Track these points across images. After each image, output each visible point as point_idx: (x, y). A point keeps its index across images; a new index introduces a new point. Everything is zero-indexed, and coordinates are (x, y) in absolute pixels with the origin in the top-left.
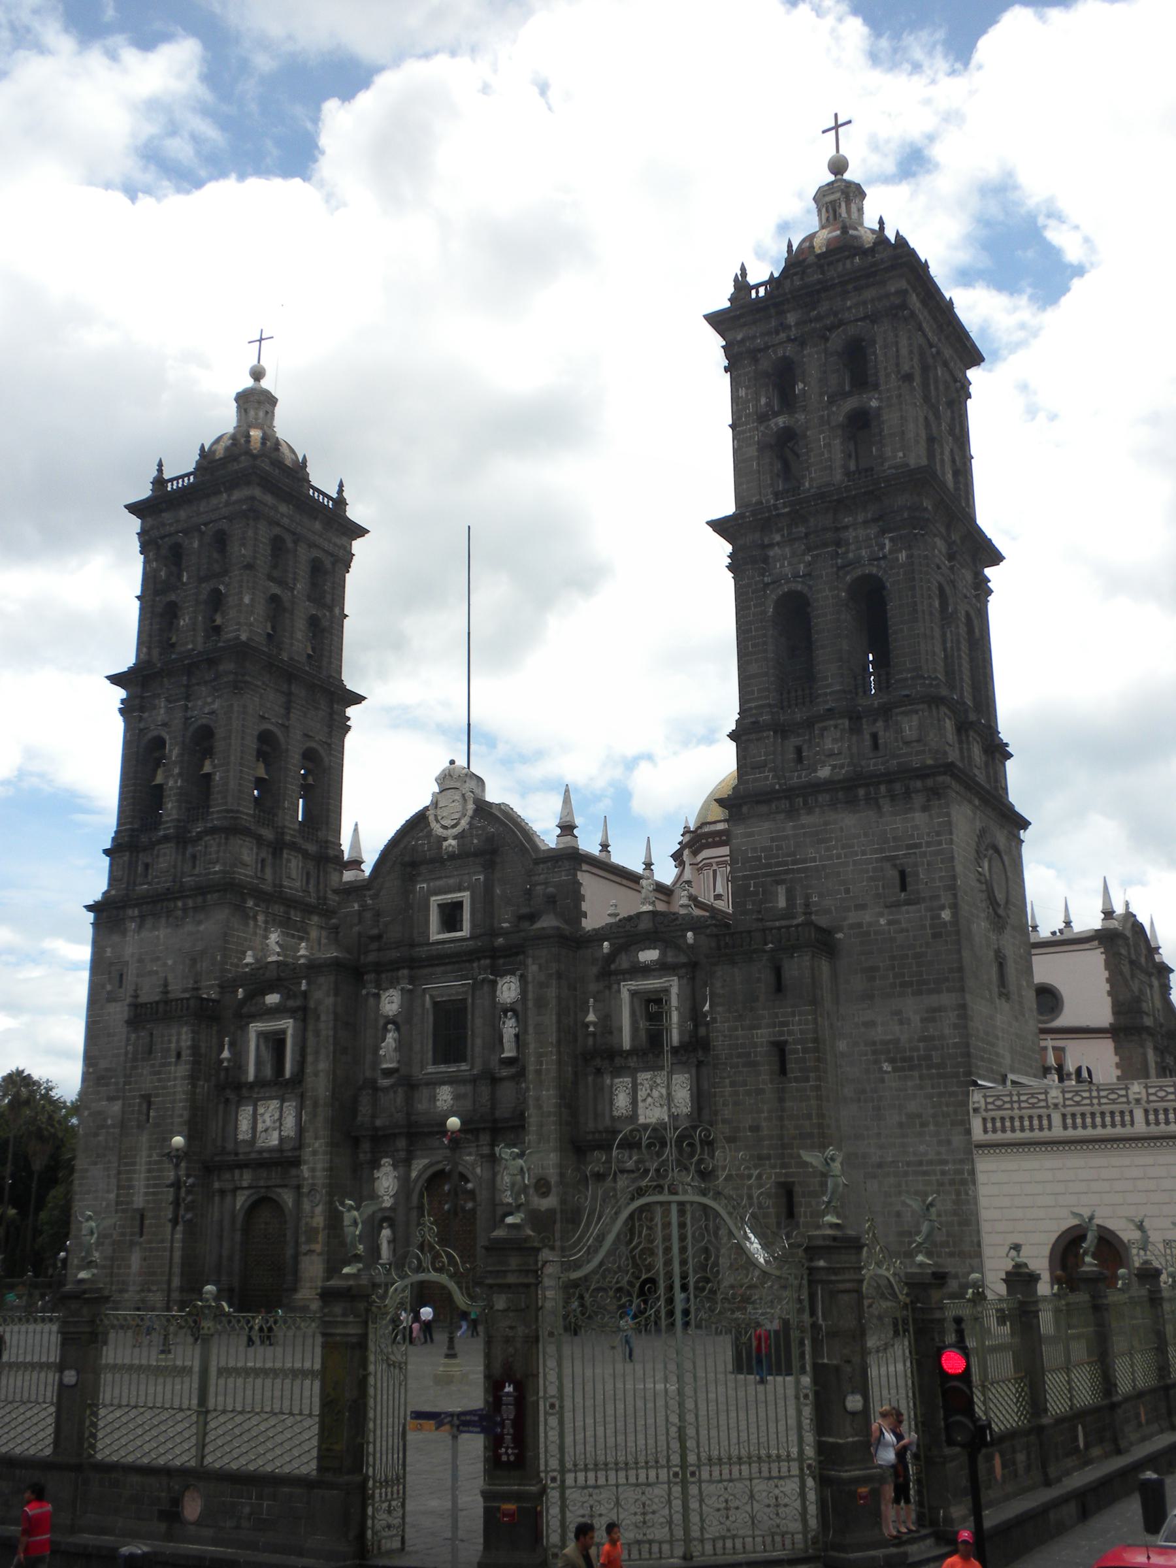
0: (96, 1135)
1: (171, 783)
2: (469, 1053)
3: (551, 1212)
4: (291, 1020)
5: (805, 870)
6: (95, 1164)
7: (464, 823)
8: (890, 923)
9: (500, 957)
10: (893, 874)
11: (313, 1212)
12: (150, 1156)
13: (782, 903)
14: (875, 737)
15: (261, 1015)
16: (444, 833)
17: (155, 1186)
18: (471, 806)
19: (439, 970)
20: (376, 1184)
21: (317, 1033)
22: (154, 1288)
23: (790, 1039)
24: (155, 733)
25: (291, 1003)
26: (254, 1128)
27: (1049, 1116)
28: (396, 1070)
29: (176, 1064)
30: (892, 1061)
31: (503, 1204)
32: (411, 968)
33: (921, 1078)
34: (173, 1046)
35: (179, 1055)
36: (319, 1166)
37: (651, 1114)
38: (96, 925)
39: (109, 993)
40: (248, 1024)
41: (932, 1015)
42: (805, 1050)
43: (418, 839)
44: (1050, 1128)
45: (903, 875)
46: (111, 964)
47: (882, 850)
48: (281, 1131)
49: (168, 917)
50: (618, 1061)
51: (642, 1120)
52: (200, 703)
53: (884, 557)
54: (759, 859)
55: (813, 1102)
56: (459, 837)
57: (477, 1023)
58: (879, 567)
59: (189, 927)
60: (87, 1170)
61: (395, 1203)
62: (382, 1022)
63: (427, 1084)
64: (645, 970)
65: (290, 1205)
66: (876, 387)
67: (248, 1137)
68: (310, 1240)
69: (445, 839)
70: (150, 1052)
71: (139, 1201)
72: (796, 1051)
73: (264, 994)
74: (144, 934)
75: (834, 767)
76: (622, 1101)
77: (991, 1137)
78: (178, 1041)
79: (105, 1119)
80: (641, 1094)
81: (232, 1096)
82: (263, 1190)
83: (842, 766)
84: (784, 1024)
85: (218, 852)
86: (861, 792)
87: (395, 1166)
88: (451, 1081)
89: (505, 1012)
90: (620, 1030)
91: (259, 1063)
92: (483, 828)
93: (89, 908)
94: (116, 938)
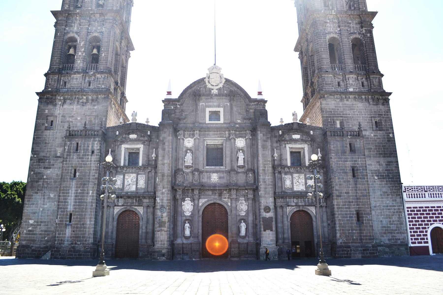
0: (37, 182)
1: (80, 54)
2: (224, 163)
3: (271, 218)
4: (143, 145)
5: (347, 117)
6: (37, 193)
7: (221, 86)
8: (374, 136)
9: (237, 131)
10: (374, 122)
11: (162, 215)
13: (338, 126)
14: (363, 83)
16: (212, 87)
17: (79, 202)
18: (224, 81)
19: (211, 133)
20: (183, 207)
21: (164, 149)
22: (79, 243)
23: (358, 166)
25: (142, 138)
27: (424, 194)
28: (192, 167)
29: (91, 156)
30: (377, 176)
31: (239, 215)
32: (200, 131)
33: (387, 181)
34: (90, 148)
35: (93, 152)
36: (165, 199)
37: (299, 187)
38: (40, 101)
39: (46, 127)
40: (121, 144)
41: (389, 163)
42: (363, 169)
43: (200, 88)
44: (425, 197)
45: (376, 122)
46: (47, 116)
47: (371, 115)
48: (137, 185)
50: (287, 170)
51: (295, 189)
52: (94, 28)
53: (363, 34)
54: (331, 112)
55: (366, 185)
56: (219, 89)
57: (227, 153)
58: (361, 36)
59: (88, 106)
60: (32, 195)
61: (192, 214)
62: (184, 149)
63: (207, 172)
64: (296, 141)
65: (142, 213)
67: (121, 187)
68: (160, 226)
69: (212, 89)
70: (77, 150)
71: (70, 208)
72: (360, 170)
73: (129, 134)
74: (66, 106)
75: (354, 89)
76: (288, 183)
77: (408, 200)
79: (43, 176)
80: (295, 181)
81: (114, 172)
82: (128, 207)
83: (356, 89)
84: (356, 161)
85: (103, 81)
86: (363, 97)
87: (193, 200)
89: (240, 150)
90: (286, 160)
91: (125, 160)
92: (228, 88)
93: (38, 94)
94: (50, 107)
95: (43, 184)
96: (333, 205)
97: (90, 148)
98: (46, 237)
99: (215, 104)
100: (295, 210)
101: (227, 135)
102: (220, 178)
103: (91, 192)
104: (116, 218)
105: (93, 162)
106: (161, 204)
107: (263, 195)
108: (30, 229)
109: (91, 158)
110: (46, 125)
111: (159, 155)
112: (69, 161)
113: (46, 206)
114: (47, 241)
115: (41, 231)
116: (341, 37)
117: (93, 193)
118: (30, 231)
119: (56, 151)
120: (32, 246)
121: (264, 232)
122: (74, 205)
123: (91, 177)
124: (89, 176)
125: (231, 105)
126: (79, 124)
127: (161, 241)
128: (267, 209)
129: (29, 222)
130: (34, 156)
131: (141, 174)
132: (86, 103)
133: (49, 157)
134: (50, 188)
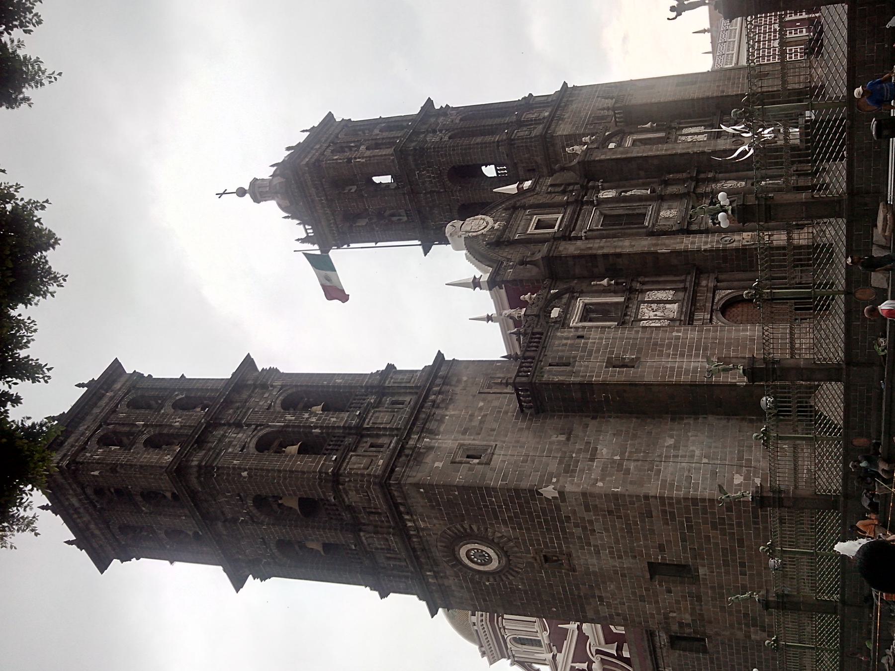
0: (628, 471)
7: (488, 219)
15: (565, 318)
16: (489, 227)
17: (698, 349)
24: (254, 441)
25: (564, 301)
34: (569, 342)
35: (581, 337)
49: (438, 407)
59: (458, 390)
60: (664, 481)
66: (378, 124)
69: (493, 227)
78: (567, 338)
79: (614, 461)
88: (659, 212)
94: (428, 459)
95: (638, 460)
99: (522, 223)
101: (589, 207)
102: (670, 209)
103: (674, 334)
111: (612, 251)
113: (697, 453)
116: (453, 130)
117: (678, 331)
120: (809, 470)
125: (530, 207)
126: (496, 403)
133: (565, 453)
134: (648, 446)
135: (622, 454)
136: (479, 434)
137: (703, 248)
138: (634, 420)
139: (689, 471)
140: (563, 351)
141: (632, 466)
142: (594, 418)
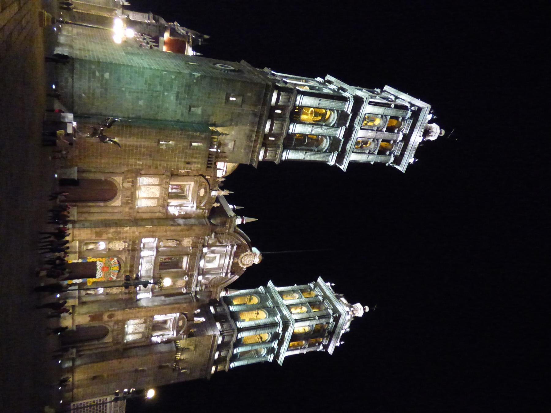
6: (146, 84)
7: (241, 265)
11: (109, 233)
12: (144, 147)
16: (240, 258)
17: (129, 150)
22: (77, 151)
26: (149, 185)
29: (184, 162)
36: (128, 235)
56: (237, 263)
62: (181, 239)
73: (205, 189)
74: (250, 118)
78: (195, 163)
79: (167, 91)
96: (112, 360)
97: (194, 160)
98: (85, 94)
100: (110, 329)
103: (141, 163)
104: (108, 179)
105: (176, 164)
106: (122, 231)
107: (126, 312)
108: (97, 74)
109: (181, 162)
110: (232, 94)
112: (181, 138)
114: (80, 97)
115: (94, 90)
117: (139, 165)
118: (94, 73)
119: (197, 106)
121: (88, 315)
122: (125, 146)
123: (159, 162)
124: (161, 160)
127: (80, 234)
128: (111, 316)
129: (106, 72)
130: (195, 78)
131: (158, 202)
132: (250, 139)
135: (164, 94)
136: (232, 113)
137: (128, 228)
138: (159, 118)
139: (131, 83)
140: (196, 154)
141: (159, 88)
142: (178, 121)
